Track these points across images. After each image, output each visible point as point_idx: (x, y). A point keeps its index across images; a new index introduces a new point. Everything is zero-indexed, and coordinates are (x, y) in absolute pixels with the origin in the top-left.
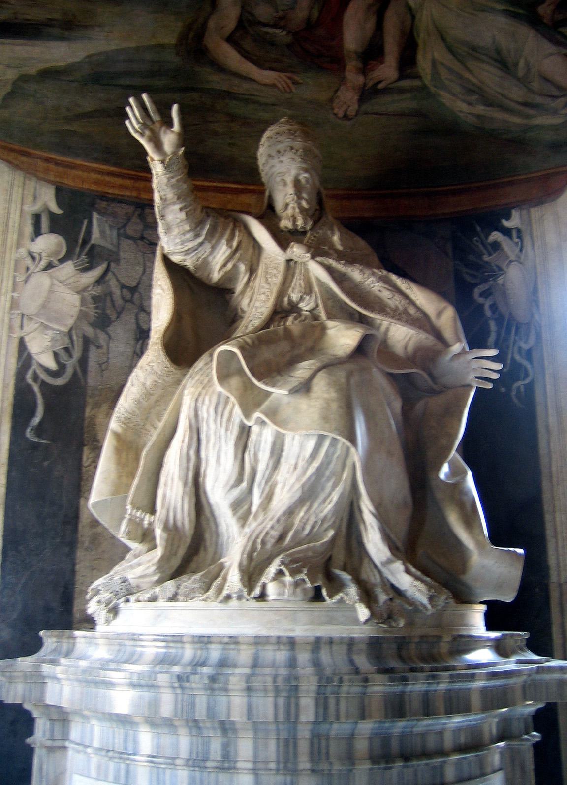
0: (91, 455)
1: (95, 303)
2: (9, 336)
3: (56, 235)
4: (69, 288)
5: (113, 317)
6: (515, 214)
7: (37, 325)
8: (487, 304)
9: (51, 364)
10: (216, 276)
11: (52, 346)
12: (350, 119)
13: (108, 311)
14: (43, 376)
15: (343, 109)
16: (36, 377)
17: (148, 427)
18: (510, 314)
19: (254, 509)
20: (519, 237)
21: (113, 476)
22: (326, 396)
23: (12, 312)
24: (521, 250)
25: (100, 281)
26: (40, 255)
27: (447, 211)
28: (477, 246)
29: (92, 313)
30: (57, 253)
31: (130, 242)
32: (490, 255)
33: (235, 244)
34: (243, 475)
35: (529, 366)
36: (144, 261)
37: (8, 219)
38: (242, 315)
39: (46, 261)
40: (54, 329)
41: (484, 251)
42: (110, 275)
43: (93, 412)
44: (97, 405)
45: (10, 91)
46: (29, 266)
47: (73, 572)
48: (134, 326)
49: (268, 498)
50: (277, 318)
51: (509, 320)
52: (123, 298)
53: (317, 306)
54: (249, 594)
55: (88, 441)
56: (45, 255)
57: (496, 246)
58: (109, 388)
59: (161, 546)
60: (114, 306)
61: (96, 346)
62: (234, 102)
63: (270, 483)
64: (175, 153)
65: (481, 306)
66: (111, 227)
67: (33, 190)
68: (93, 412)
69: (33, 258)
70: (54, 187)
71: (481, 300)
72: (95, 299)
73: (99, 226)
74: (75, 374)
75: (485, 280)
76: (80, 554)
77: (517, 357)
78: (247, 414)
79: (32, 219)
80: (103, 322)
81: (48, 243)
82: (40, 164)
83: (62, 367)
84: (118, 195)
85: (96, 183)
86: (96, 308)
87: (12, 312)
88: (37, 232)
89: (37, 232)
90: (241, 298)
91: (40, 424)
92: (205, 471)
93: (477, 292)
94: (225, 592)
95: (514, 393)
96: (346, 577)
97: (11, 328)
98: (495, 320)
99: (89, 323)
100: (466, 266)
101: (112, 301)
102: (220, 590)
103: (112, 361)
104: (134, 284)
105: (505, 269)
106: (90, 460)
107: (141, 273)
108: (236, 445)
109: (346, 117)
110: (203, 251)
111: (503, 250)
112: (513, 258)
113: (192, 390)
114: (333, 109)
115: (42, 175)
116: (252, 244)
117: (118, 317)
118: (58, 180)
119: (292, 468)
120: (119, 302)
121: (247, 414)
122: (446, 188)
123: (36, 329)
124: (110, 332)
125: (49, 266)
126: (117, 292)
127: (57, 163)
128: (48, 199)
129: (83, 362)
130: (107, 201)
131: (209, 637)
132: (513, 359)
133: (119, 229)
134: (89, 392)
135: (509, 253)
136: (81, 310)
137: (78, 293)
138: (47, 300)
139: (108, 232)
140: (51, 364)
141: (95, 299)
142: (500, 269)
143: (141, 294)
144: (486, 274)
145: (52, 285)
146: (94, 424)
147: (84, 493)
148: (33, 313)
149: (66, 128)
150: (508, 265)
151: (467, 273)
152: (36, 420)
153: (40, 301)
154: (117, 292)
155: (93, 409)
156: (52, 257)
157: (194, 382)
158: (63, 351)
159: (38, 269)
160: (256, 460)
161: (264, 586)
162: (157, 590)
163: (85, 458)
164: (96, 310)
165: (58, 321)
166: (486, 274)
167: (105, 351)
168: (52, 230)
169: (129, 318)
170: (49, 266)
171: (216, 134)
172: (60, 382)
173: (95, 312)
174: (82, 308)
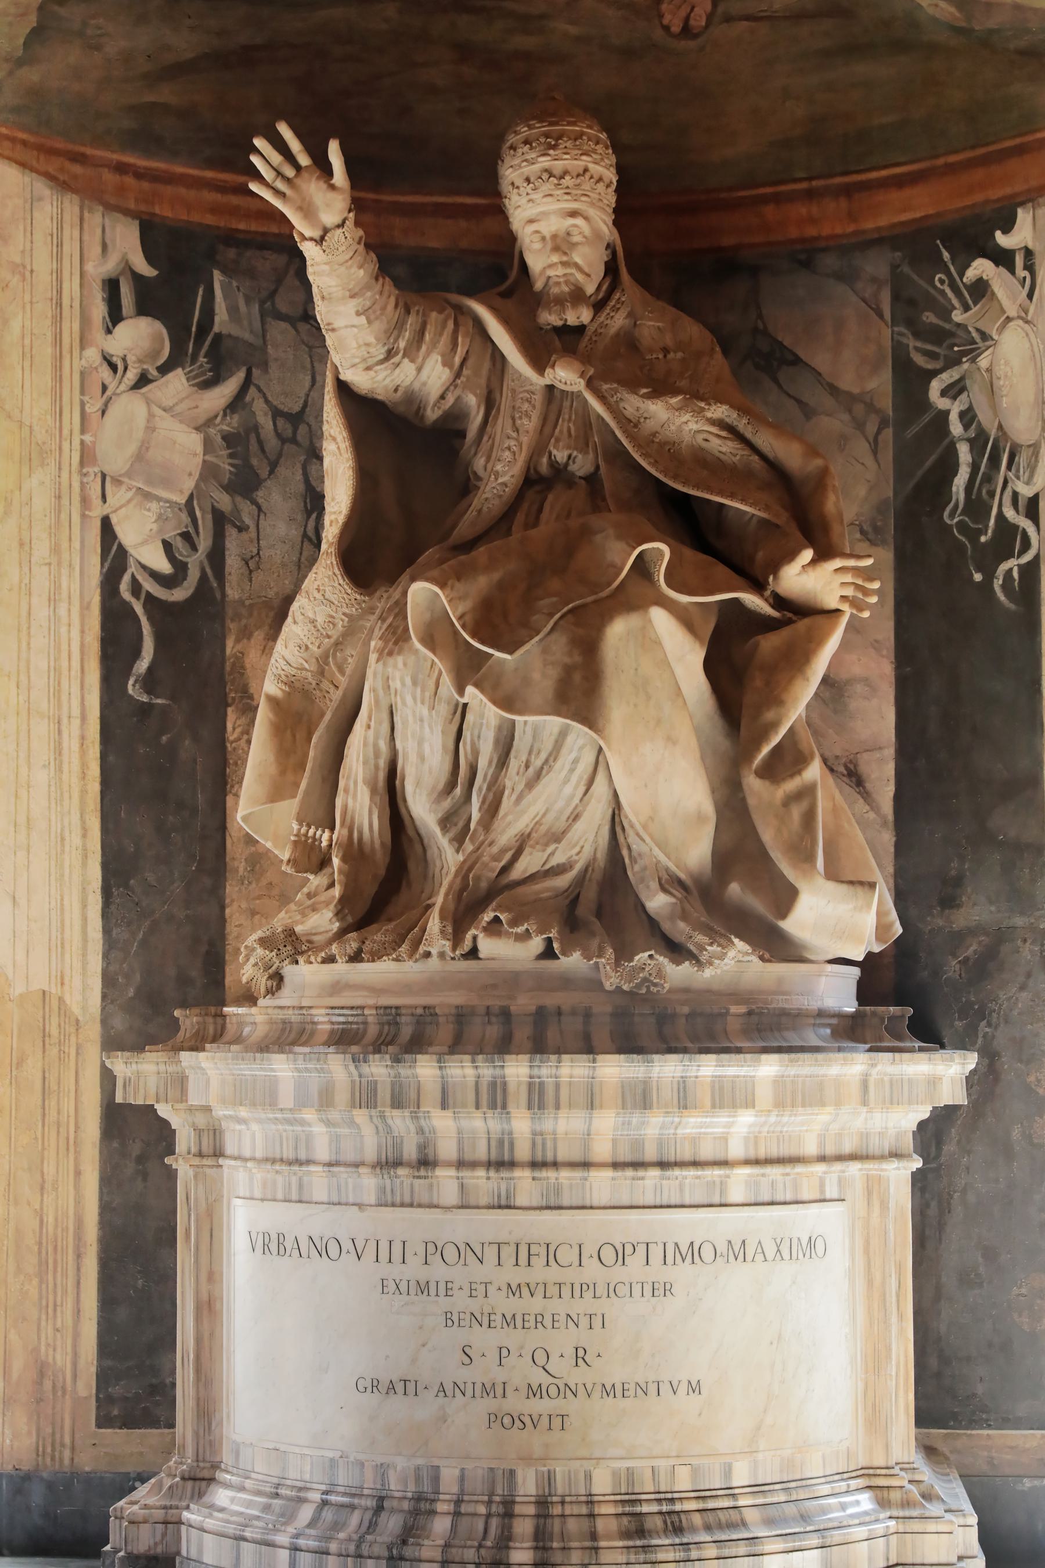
0: (238, 722)
2: (83, 516)
3: (149, 319)
4: (181, 422)
5: (264, 473)
6: (1023, 217)
7: (130, 494)
8: (955, 409)
9: (164, 566)
11: (160, 531)
12: (696, 36)
13: (254, 462)
14: (149, 586)
15: (683, 13)
16: (136, 588)
17: (326, 685)
18: (1000, 427)
19: (472, 826)
20: (1030, 267)
21: (273, 770)
22: (567, 660)
23: (84, 471)
24: (1030, 296)
25: (236, 404)
26: (124, 359)
27: (883, 221)
28: (943, 293)
29: (226, 466)
30: (155, 354)
31: (284, 325)
32: (966, 308)
33: (457, 360)
35: (1031, 530)
36: (312, 362)
37: (60, 292)
38: (478, 483)
39: (135, 371)
40: (159, 499)
41: (955, 302)
42: (252, 391)
44: (246, 634)
45: (35, 25)
46: (106, 383)
47: (222, 920)
48: (302, 487)
50: (531, 494)
51: (996, 441)
52: (278, 435)
53: (598, 468)
54: (454, 948)
55: (234, 699)
56: (134, 358)
57: (980, 289)
59: (340, 882)
60: (263, 451)
61: (235, 526)
63: (494, 789)
65: (945, 414)
66: (248, 300)
67: (99, 231)
68: (239, 647)
69: (114, 368)
70: (136, 223)
72: (228, 439)
73: (226, 297)
74: (203, 578)
75: (954, 362)
76: (231, 889)
77: (1010, 513)
79: (103, 290)
80: (245, 484)
81: (138, 336)
82: (109, 177)
83: (181, 569)
84: (256, 233)
85: (215, 209)
86: (231, 456)
87: (84, 471)
88: (115, 316)
89: (115, 316)
91: (150, 669)
92: (403, 769)
93: (936, 386)
95: (998, 583)
97: (85, 501)
98: (970, 441)
99: (222, 487)
100: (917, 335)
101: (260, 443)
104: (296, 408)
105: (995, 337)
106: (238, 730)
107: (307, 385)
109: (686, 30)
111: (993, 294)
112: (1012, 311)
114: (661, 16)
115: (113, 201)
116: (490, 351)
117: (272, 472)
118: (143, 208)
119: (523, 765)
120: (272, 443)
122: (884, 173)
123: (129, 501)
124: (260, 501)
125: (144, 380)
126: (265, 422)
127: (139, 175)
128: (126, 245)
129: (217, 556)
131: (397, 1008)
132: (1000, 515)
133: (262, 303)
134: (230, 612)
135: (1006, 303)
136: (204, 461)
137: (197, 429)
138: (144, 447)
139: (243, 307)
140: (164, 566)
141: (228, 439)
142: (985, 336)
143: (310, 426)
144: (956, 349)
145: (151, 416)
146: (243, 667)
147: (232, 786)
148: (123, 472)
149: (150, 98)
150: (1003, 326)
151: (916, 349)
152: (143, 665)
153: (132, 449)
154: (265, 422)
155: (238, 641)
156: (144, 363)
157: (385, 626)
158: (179, 538)
159: (123, 387)
160: (476, 753)
162: (334, 949)
163: (229, 726)
164: (230, 461)
165: (166, 482)
166: (956, 349)
167: (254, 535)
168: (143, 309)
169: (291, 474)
170: (144, 380)
172: (179, 595)
173: (230, 464)
174: (207, 458)
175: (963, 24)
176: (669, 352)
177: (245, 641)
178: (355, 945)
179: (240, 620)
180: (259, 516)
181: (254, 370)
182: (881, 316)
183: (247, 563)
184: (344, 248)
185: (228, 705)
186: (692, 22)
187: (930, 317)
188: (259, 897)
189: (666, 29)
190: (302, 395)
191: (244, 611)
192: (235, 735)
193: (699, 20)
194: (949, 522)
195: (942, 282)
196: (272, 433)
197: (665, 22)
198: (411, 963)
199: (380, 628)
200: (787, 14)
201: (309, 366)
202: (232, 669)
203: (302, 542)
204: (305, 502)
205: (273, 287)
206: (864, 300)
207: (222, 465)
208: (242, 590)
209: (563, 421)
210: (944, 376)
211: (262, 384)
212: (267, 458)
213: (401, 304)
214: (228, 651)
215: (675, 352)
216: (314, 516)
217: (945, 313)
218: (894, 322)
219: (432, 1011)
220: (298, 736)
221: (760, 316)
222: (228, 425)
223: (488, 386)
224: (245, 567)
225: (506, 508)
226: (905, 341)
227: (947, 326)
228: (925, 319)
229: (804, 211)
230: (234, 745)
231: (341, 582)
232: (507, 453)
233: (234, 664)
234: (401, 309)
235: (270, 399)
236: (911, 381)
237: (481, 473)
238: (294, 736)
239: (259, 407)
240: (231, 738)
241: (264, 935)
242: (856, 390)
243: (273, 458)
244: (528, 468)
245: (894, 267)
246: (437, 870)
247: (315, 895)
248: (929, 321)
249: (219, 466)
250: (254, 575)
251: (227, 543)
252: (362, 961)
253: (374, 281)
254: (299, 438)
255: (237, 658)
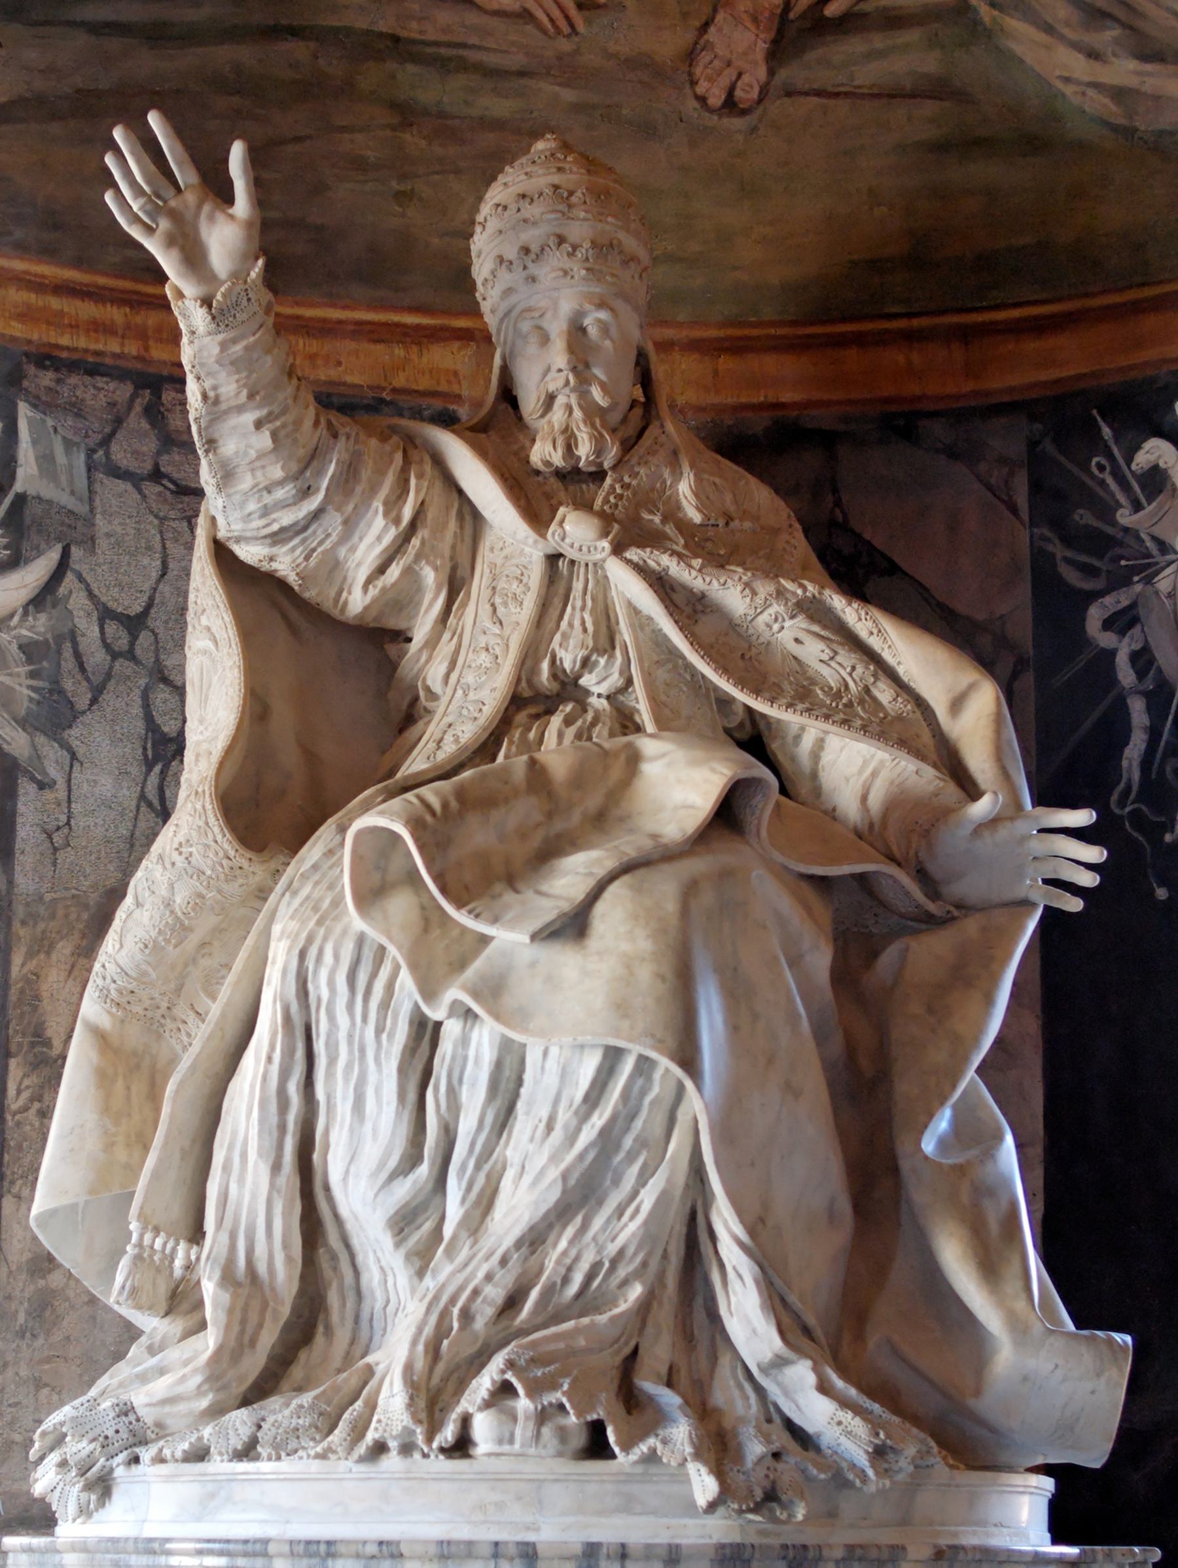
0: (26, 1082)
1: (30, 660)
5: (82, 702)
10: (357, 601)
12: (744, 112)
13: (68, 685)
17: (181, 1011)
19: (448, 1230)
21: (92, 1144)
22: (625, 947)
27: (1015, 380)
28: (1102, 483)
32: (1137, 507)
33: (407, 512)
34: (422, 1143)
36: (163, 540)
38: (430, 705)
41: (1121, 497)
42: (69, 578)
43: (32, 965)
44: (43, 946)
48: (140, 726)
49: (484, 1204)
50: (521, 717)
52: (107, 646)
53: (629, 682)
54: (429, 1439)
55: (20, 1045)
58: (74, 896)
59: (215, 1324)
60: (82, 669)
61: (33, 779)
62: (411, 68)
63: (487, 1167)
64: (238, 275)
65: (1110, 655)
66: (68, 444)
68: (32, 965)
71: (1106, 640)
73: (35, 442)
75: (1121, 581)
78: (429, 992)
84: (86, 351)
85: (26, 315)
86: (32, 675)
90: (424, 658)
93: (1095, 615)
94: (371, 1436)
96: (670, 1399)
98: (1148, 695)
100: (1067, 541)
101: (78, 655)
102: (359, 1431)
103: (79, 823)
104: (137, 608)
106: (25, 1095)
107: (155, 575)
108: (403, 1071)
109: (730, 105)
110: (319, 532)
113: (294, 925)
114: (694, 83)
117: (94, 701)
119: (542, 1126)
120: (96, 657)
121: (429, 992)
122: (1016, 313)
124: (75, 744)
130: (57, 370)
131: (329, 1543)
133: (91, 452)
134: (20, 911)
143: (156, 635)
144: (1123, 563)
146: (37, 998)
147: (12, 1182)
151: (1066, 560)
155: (30, 955)
157: (296, 902)
161: (466, 1421)
166: (1123, 563)
167: (62, 794)
169: (123, 703)
171: (359, 165)
173: (30, 687)
175: (1121, 121)
176: (732, 520)
177: (42, 956)
178: (245, 1432)
179: (35, 924)
180: (71, 766)
181: (73, 549)
182: (1014, 511)
183: (50, 837)
184: (244, 316)
185: (8, 1055)
186: (738, 93)
187: (1083, 517)
188: (48, 1360)
189: (702, 100)
190: (147, 586)
191: (42, 910)
192: (21, 1102)
193: (747, 93)
194: (1117, 811)
195: (1101, 468)
196: (99, 642)
197: (700, 89)
198: (349, 1464)
199: (289, 904)
200: (876, 91)
201: (158, 547)
202: (19, 999)
203: (138, 808)
204: (145, 749)
205: (108, 430)
206: (989, 487)
207: (17, 687)
208: (41, 878)
209: (574, 608)
210: (1108, 600)
211: (84, 569)
212: (88, 680)
213: (323, 421)
214: (15, 971)
215: (741, 520)
216: (157, 769)
217: (1107, 511)
218: (1032, 523)
219: (394, 1549)
220: (134, 1089)
221: (838, 503)
222: (31, 629)
223: (452, 558)
224: (47, 844)
225: (486, 735)
226: (1050, 548)
227: (1110, 530)
228: (1077, 517)
229: (901, 358)
230: (17, 1117)
231: (219, 838)
232: (484, 655)
233: (22, 991)
234: (322, 429)
235: (96, 592)
236: (1059, 607)
237: (437, 688)
238: (128, 1088)
239: (78, 602)
240: (14, 1107)
241: (74, 1413)
242: (981, 616)
243: (97, 680)
244: (519, 680)
245: (1033, 444)
246: (379, 1305)
247: (161, 1349)
248: (1083, 522)
249: (13, 689)
250: (61, 855)
251: (20, 805)
252: (257, 1458)
253: (286, 379)
254: (138, 651)
255: (28, 981)
